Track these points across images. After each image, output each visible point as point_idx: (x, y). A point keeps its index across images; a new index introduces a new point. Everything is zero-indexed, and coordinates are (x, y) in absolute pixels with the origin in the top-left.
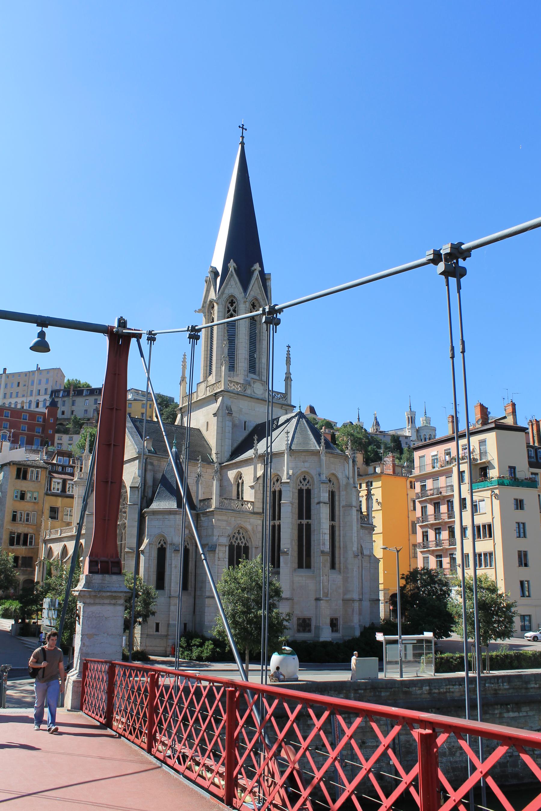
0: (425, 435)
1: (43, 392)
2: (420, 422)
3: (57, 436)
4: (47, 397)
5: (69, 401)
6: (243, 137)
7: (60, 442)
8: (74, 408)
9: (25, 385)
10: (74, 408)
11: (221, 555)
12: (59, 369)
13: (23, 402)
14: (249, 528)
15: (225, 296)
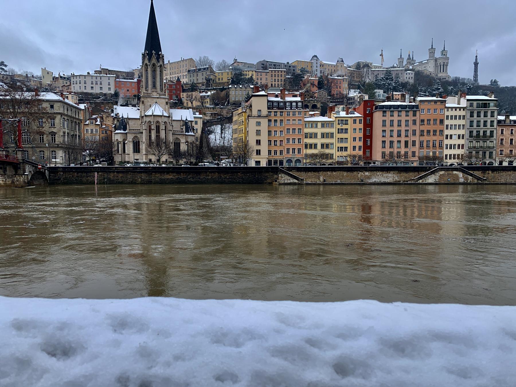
0: (440, 63)
2: (438, 55)
4: (187, 73)
7: (183, 96)
8: (198, 78)
9: (178, 68)
10: (198, 78)
11: (130, 144)
12: (191, 59)
14: (139, 136)
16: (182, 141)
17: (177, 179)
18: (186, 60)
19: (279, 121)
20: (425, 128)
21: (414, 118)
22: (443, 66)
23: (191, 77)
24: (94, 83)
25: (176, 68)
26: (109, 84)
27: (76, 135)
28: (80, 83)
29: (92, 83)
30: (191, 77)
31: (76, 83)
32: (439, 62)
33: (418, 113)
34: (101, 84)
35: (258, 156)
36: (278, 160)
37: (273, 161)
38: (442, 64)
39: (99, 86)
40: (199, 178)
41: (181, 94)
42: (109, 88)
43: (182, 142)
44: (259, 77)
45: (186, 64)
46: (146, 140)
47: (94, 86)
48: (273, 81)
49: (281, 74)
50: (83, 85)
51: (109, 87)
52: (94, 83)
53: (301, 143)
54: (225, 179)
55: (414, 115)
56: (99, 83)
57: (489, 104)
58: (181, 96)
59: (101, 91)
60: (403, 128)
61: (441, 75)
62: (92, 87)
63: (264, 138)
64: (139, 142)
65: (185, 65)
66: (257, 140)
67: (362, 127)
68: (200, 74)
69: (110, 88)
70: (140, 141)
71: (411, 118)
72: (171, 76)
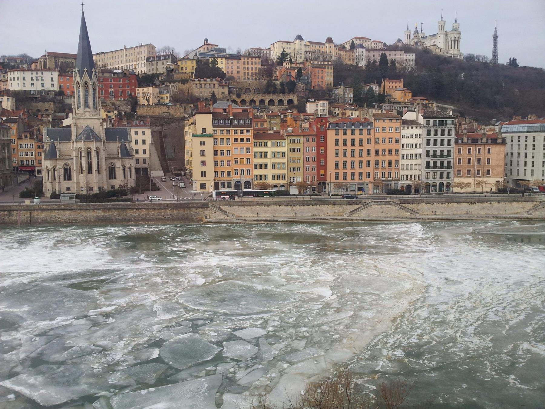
1: (143, 58)
2: (448, 28)
3: (136, 89)
4: (145, 61)
5: (155, 63)
6: (83, 9)
7: (138, 92)
8: (158, 67)
10: (158, 67)
13: (135, 65)
15: (76, 82)
16: (117, 166)
17: (103, 216)
18: (144, 46)
19: (225, 140)
20: (380, 147)
21: (368, 137)
22: (455, 41)
23: (149, 65)
24: (35, 79)
25: (133, 55)
26: (52, 80)
27: (5, 158)
28: (18, 79)
29: (32, 79)
30: (149, 65)
31: (14, 80)
32: (449, 36)
33: (372, 132)
34: (42, 80)
35: (203, 179)
36: (226, 182)
37: (220, 183)
38: (453, 39)
39: (40, 82)
40: (126, 216)
41: (136, 89)
42: (52, 84)
43: (117, 166)
44: (230, 65)
45: (144, 51)
46: (77, 167)
47: (34, 82)
48: (247, 69)
49: (255, 61)
50: (21, 82)
51: (52, 83)
52: (35, 79)
53: (251, 163)
54: (152, 216)
55: (369, 134)
56: (40, 79)
57: (446, 121)
58: (137, 92)
59: (43, 88)
60: (357, 148)
61: (452, 52)
62: (32, 84)
63: (209, 158)
64: (70, 168)
65: (143, 52)
66: (201, 162)
67: (316, 146)
68: (160, 63)
69: (53, 85)
70: (71, 167)
71: (365, 137)
72: (128, 64)
